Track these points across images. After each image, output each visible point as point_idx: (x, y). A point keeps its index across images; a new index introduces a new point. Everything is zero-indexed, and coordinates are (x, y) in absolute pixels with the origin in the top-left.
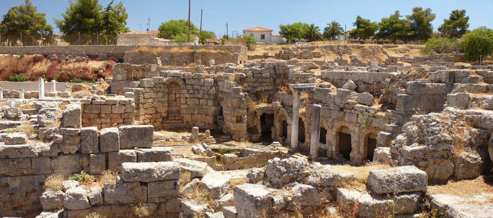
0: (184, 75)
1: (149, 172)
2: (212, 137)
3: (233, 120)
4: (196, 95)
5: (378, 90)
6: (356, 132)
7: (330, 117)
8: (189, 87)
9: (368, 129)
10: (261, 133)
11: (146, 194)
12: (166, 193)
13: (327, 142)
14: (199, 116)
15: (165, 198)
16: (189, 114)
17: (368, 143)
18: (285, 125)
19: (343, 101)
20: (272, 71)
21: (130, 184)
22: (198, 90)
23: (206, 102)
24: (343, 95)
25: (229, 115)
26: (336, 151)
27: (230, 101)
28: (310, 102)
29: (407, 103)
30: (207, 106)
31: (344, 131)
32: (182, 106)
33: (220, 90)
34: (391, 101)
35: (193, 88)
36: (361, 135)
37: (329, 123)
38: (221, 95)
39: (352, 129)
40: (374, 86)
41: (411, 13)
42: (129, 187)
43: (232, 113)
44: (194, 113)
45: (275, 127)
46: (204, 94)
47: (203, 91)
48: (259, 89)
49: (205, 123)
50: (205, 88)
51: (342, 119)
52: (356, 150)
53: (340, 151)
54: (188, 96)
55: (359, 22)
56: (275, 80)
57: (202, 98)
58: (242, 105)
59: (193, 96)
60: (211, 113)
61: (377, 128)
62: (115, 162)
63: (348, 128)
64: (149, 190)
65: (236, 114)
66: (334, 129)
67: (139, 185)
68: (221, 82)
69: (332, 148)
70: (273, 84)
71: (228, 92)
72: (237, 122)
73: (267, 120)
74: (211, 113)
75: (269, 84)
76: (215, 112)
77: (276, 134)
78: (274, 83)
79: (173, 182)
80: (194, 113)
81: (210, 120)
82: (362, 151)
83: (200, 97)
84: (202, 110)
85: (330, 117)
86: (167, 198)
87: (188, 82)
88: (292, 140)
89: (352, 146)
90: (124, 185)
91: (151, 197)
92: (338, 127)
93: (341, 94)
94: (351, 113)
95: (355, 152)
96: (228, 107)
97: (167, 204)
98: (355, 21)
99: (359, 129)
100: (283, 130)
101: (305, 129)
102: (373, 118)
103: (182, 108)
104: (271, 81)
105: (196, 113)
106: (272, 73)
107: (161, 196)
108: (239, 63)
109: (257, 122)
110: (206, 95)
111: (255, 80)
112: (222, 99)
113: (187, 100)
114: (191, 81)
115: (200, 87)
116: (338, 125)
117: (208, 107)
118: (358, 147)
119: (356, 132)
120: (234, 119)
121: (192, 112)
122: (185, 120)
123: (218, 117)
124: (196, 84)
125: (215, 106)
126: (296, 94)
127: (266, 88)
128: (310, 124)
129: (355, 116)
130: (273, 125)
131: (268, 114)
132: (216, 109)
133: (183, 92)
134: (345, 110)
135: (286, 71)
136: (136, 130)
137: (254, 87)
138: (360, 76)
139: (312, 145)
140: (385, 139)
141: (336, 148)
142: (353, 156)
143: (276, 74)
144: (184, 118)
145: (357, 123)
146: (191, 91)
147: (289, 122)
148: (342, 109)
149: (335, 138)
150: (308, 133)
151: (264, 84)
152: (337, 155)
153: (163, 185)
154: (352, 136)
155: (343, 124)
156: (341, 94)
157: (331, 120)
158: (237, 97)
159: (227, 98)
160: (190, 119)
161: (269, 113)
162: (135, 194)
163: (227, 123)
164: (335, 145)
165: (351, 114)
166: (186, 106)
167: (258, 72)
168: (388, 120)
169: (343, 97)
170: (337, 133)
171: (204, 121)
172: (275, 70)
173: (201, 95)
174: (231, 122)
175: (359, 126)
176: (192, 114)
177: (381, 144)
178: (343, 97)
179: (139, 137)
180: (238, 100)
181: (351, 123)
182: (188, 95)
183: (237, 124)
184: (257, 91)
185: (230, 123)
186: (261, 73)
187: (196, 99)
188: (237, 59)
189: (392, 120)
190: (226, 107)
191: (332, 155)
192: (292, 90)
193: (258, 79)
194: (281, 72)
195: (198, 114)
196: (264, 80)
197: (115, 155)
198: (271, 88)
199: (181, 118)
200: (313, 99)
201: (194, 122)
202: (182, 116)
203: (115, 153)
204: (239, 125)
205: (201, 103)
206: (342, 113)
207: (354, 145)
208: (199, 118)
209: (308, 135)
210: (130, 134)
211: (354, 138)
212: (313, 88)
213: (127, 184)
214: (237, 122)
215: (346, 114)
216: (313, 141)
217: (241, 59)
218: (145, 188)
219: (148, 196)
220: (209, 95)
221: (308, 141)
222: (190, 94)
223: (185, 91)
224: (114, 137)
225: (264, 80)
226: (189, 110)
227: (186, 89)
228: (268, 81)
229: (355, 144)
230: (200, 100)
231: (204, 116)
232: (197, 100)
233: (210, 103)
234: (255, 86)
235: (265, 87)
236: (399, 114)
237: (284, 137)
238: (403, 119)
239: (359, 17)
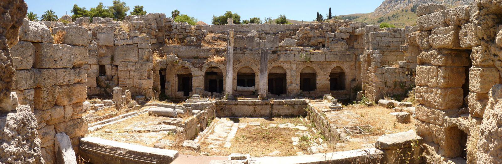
9: (304, 64)
24: (275, 40)
41: (112, 5)
52: (294, 83)
55: (76, 10)
68: (103, 35)
98: (72, 9)
102: (311, 55)
129: (293, 55)
138: (258, 28)
215: (282, 55)
239: (75, 6)
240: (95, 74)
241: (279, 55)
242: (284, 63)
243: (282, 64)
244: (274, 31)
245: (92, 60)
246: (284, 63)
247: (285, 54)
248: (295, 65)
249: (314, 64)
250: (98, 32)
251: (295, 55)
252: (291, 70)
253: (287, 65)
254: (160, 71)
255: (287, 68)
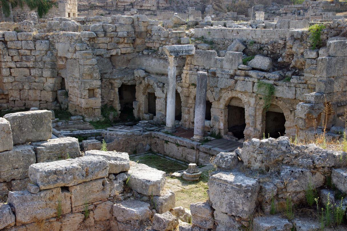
0: (3, 35)
1: (69, 171)
2: (58, 119)
3: (84, 95)
4: (24, 64)
5: (274, 52)
6: (252, 105)
7: (217, 87)
8: (13, 52)
10: (120, 111)
11: (69, 202)
12: (94, 196)
13: (212, 118)
14: (31, 92)
15: (92, 203)
16: (16, 90)
17: (266, 117)
18: (152, 98)
19: (234, 66)
20: (130, 29)
21: (49, 192)
22: (26, 55)
23: (40, 72)
24: (234, 59)
25: (78, 89)
26: (224, 129)
27: (77, 69)
28: (188, 69)
29: (331, 67)
30: (42, 78)
31: (234, 103)
32: (5, 80)
33: (59, 55)
34: (296, 64)
35: (19, 54)
36: (258, 107)
37: (214, 93)
38: (60, 63)
39: (246, 100)
40: (269, 47)
42: (48, 196)
43: (83, 85)
44: (23, 89)
45: (137, 101)
46: (36, 61)
47: (34, 57)
48: (114, 53)
49: (40, 101)
50: (37, 53)
51: (232, 89)
52: (252, 127)
53: (228, 128)
54: (13, 65)
56: (134, 40)
57: (34, 68)
58: (95, 75)
59: (20, 65)
60: (49, 87)
61: (278, 99)
62: (8, 166)
63: (240, 99)
64: (73, 197)
65: (88, 87)
66: (222, 101)
67: (61, 192)
69: (219, 125)
70: (132, 45)
71: (74, 57)
72: (89, 97)
73: (127, 95)
74: (49, 87)
75: (126, 45)
76: (54, 86)
77: (139, 110)
78: (132, 43)
79: (101, 182)
80: (23, 89)
81: (49, 96)
82: (259, 127)
83: (31, 66)
84: (35, 83)
85: (217, 87)
86: (95, 203)
87: (10, 45)
88: (167, 117)
89: (247, 121)
90: (42, 195)
91: (76, 205)
92: (227, 99)
93: (231, 57)
94: (244, 80)
95: (251, 129)
96: (76, 78)
97: (97, 211)
99: (256, 101)
100: (149, 105)
101: (181, 102)
103: (4, 82)
104: (129, 42)
105: (27, 88)
106: (129, 31)
107: (88, 202)
108: (67, 16)
109: (114, 96)
110: (40, 63)
111: (109, 40)
112: (64, 67)
113: (12, 70)
114: (14, 44)
115: (30, 51)
116: (227, 96)
117: (44, 79)
118: (254, 123)
119: (252, 105)
120: (86, 93)
121: (21, 87)
122: (11, 99)
123: (59, 92)
124: (24, 48)
125: (53, 77)
126: (173, 58)
127: (124, 51)
128: (188, 97)
129: (250, 84)
130: (134, 99)
131: (129, 85)
132: (55, 81)
133: (5, 60)
134: (236, 78)
135: (149, 28)
136: (29, 118)
137: (108, 50)
138: (249, 34)
139: (197, 123)
140: (307, 111)
141: (224, 125)
142: (248, 133)
143: (135, 32)
144: (9, 97)
145: (253, 92)
146: (16, 58)
147: (158, 93)
148: (232, 77)
149: (223, 112)
150: (186, 106)
151: (120, 46)
152: (226, 133)
153: (89, 187)
154: (245, 110)
155: (234, 95)
156: (231, 57)
157: (217, 90)
158: (88, 63)
159: (72, 65)
160: (19, 97)
161: (129, 84)
162: (56, 204)
163: (74, 99)
164: (223, 121)
165: (245, 82)
166: (10, 79)
167: (112, 30)
168: (294, 88)
169: (234, 61)
170: (226, 106)
171: (39, 99)
172: (134, 27)
173: (33, 63)
174: (81, 98)
175: (255, 96)
176: (20, 90)
177: (301, 118)
178: (234, 61)
179: (33, 128)
180: (90, 68)
181: (245, 92)
182: (12, 64)
183: (90, 99)
184: (112, 56)
185: (79, 99)
186: (115, 31)
187: (24, 69)
188: (64, 11)
189: (299, 88)
190: (71, 78)
191: (220, 133)
192: (168, 54)
193: (113, 39)
194: (143, 29)
195: (30, 89)
196: (121, 40)
197: (8, 156)
198: (129, 50)
199: (4, 97)
200: (191, 64)
201: (24, 101)
202: (6, 93)
203: (7, 152)
204: (92, 100)
205: (32, 74)
206: (232, 81)
207: (248, 120)
208: (31, 95)
209: (187, 111)
210: (21, 124)
211: (248, 112)
212: (192, 50)
213: (45, 192)
214: (89, 97)
216: (197, 118)
217: (69, 11)
218: (67, 194)
219: (73, 203)
220: (45, 62)
221: (187, 118)
222: (16, 62)
223: (8, 58)
224: (5, 130)
225: (121, 40)
226: (15, 85)
227: (9, 55)
228: (126, 41)
229: (250, 119)
230: (31, 70)
231: (38, 92)
232: (27, 71)
233: (47, 73)
234: (109, 48)
235: (122, 49)
236: (321, 81)
237: (151, 114)
238: (326, 87)
240: (49, 88)
241: (236, 81)
242: (242, 94)
243: (239, 95)
244: (266, 40)
245: (47, 73)
246: (242, 94)
247: (243, 80)
248: (254, 99)
249: (280, 101)
250: (56, 41)
251: (254, 83)
252: (249, 103)
253: (245, 97)
254: (120, 89)
255: (245, 102)
